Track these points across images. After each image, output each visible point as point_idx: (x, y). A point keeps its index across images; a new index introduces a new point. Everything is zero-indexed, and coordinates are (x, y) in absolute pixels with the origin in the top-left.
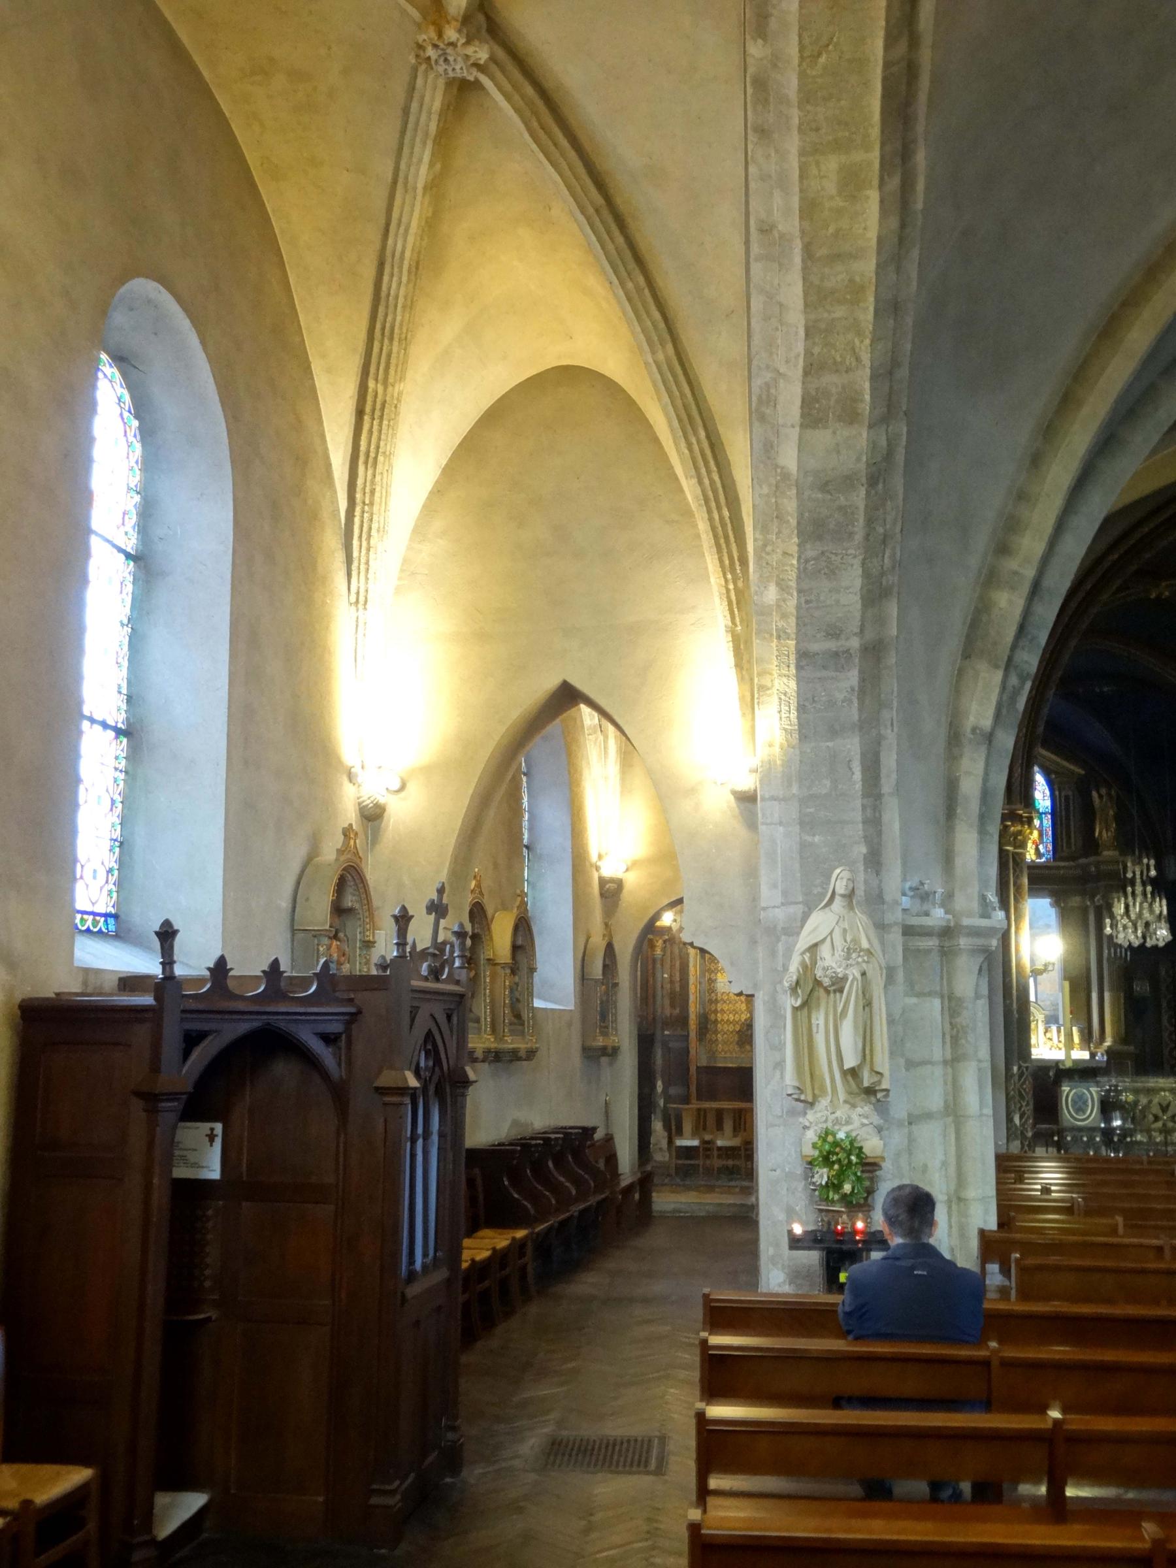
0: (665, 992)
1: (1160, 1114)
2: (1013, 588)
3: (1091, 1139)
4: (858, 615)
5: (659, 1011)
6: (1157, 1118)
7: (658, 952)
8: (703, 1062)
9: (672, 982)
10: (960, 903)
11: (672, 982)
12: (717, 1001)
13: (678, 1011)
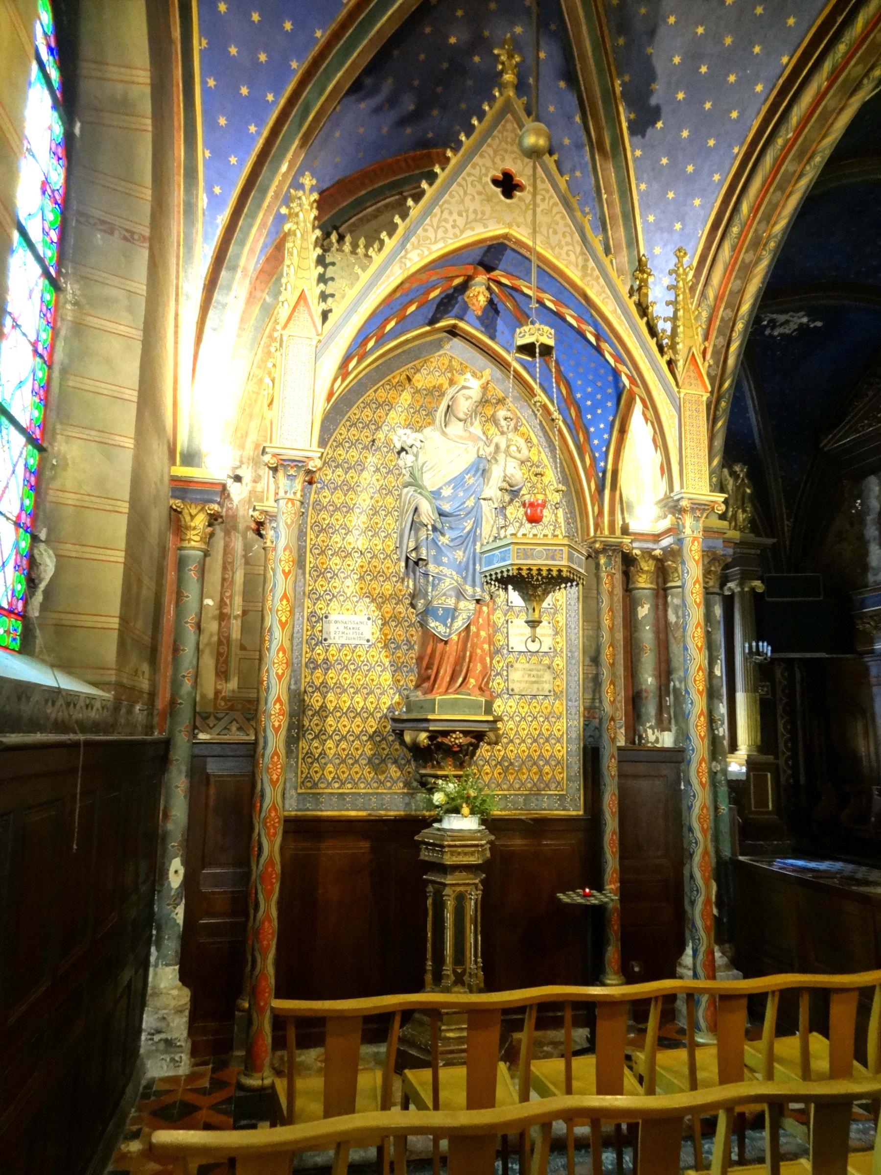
0: (204, 639)
5: (187, 685)
7: (194, 541)
8: (292, 808)
9: (222, 617)
11: (222, 617)
12: (327, 665)
13: (233, 684)
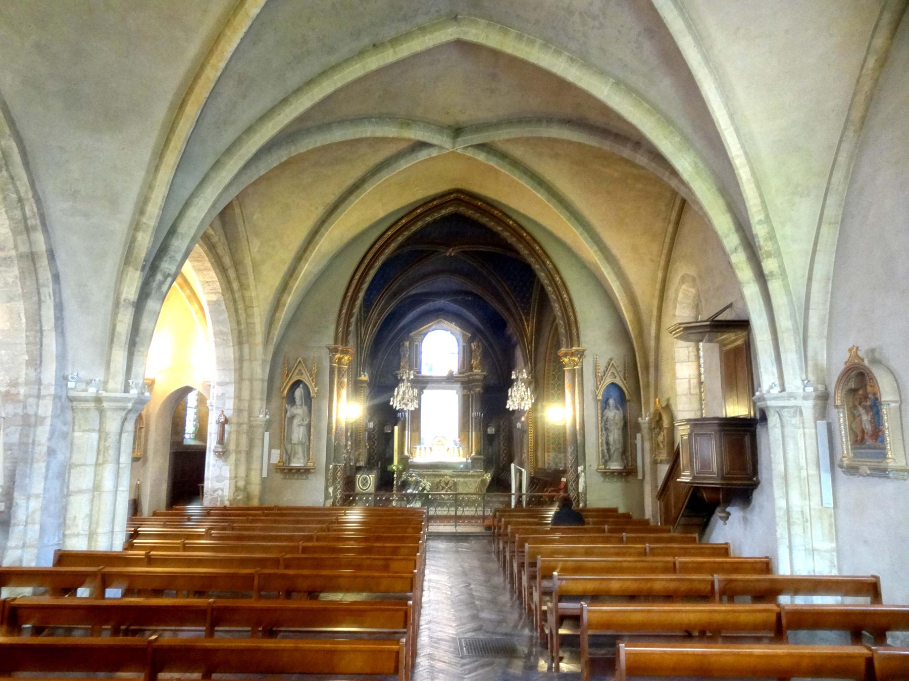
2: (144, 232)
3: (367, 499)
4: (11, 239)
6: (443, 488)
10: (111, 385)
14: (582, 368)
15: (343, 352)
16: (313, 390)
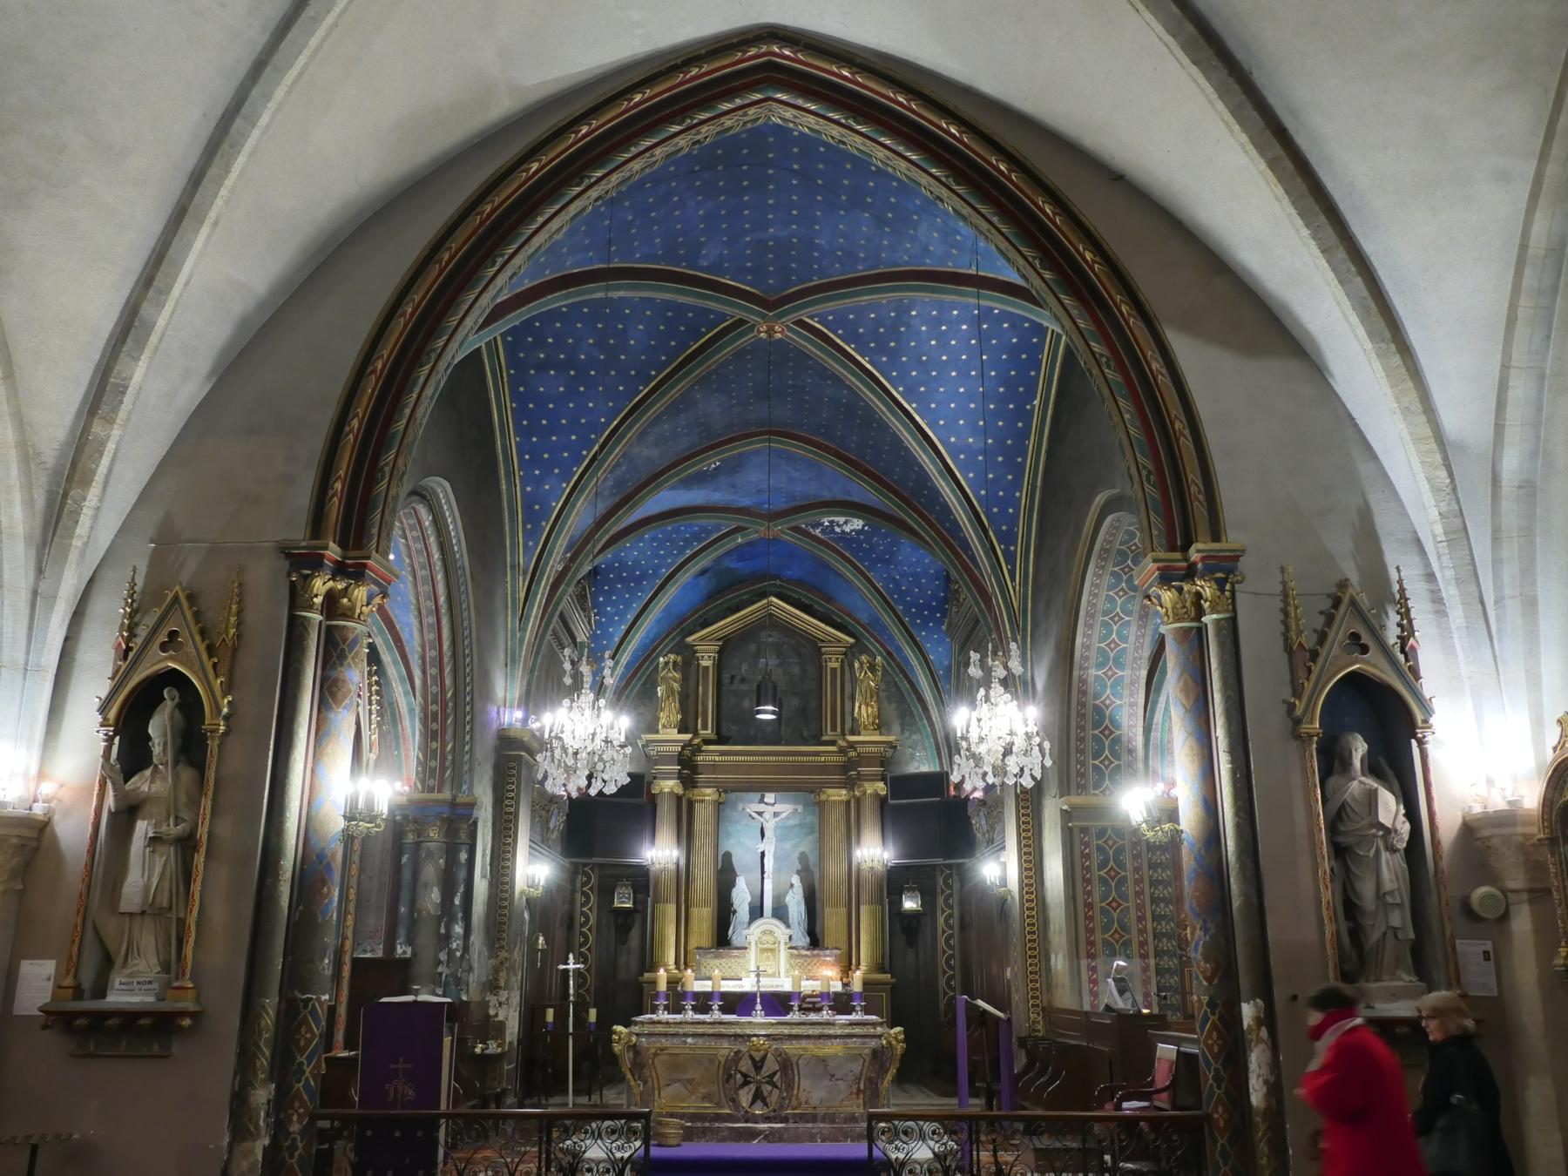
1: (753, 1073)
14: (1233, 621)
15: (340, 570)
16: (218, 704)
